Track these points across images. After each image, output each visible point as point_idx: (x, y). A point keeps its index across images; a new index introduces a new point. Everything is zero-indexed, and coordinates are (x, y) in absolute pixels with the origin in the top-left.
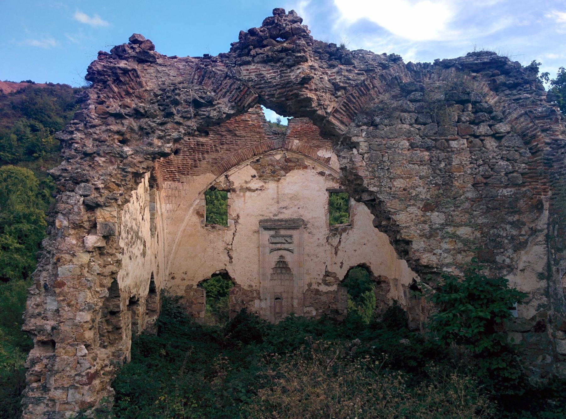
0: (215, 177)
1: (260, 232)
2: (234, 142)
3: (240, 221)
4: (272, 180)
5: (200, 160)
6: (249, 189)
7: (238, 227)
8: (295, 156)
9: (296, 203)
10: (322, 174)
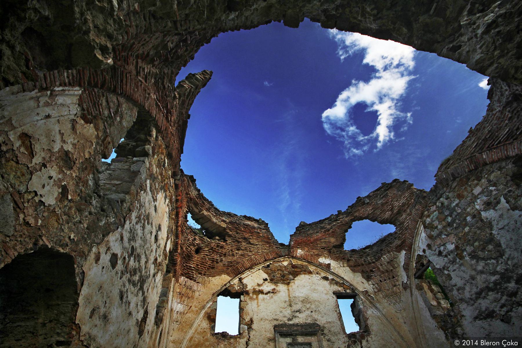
0: (230, 278)
1: (277, 339)
2: (248, 249)
3: (254, 326)
4: (282, 283)
5: (217, 262)
6: (261, 292)
7: (252, 333)
8: (300, 262)
9: (308, 306)
10: (326, 278)
